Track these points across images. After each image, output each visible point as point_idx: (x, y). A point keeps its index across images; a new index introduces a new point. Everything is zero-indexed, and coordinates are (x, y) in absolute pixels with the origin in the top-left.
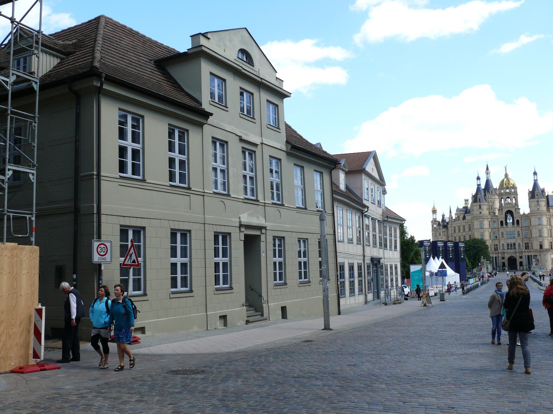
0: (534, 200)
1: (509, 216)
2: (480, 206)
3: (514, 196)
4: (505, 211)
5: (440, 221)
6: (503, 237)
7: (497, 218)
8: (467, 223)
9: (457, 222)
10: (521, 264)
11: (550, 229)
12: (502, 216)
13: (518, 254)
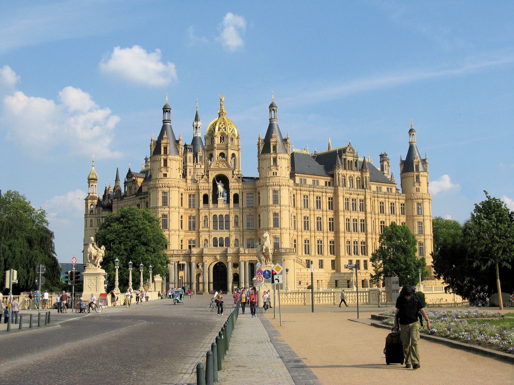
0: (267, 156)
1: (220, 188)
2: (165, 161)
3: (232, 152)
4: (212, 175)
5: (101, 198)
6: (206, 225)
7: (198, 189)
8: (143, 200)
9: (127, 198)
10: (236, 278)
11: (295, 215)
12: (207, 185)
13: (229, 258)
